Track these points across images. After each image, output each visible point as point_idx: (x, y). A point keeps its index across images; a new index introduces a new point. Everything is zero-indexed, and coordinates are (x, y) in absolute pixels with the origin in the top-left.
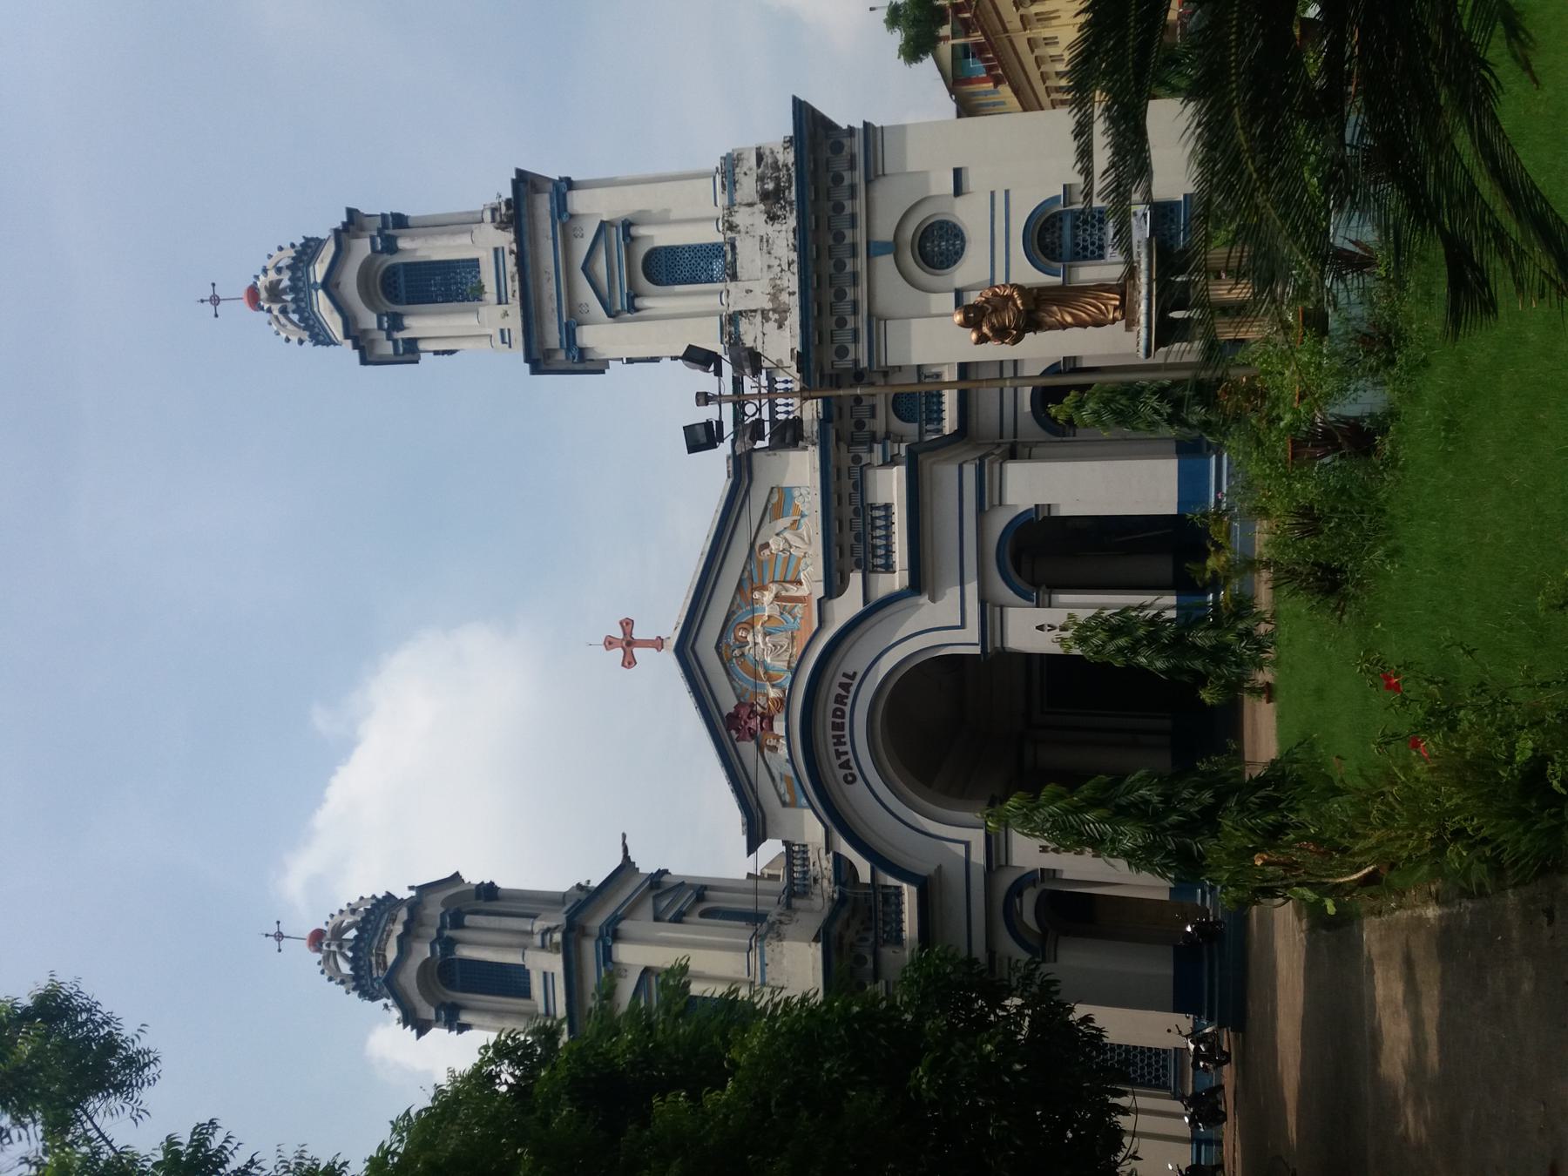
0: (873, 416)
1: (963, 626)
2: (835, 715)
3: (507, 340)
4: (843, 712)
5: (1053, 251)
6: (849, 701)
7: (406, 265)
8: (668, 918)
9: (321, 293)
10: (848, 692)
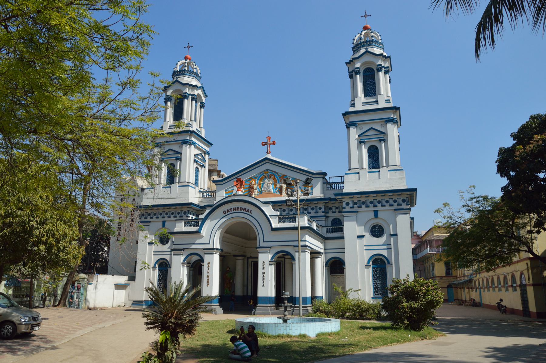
0: (333, 212)
1: (264, 242)
2: (241, 208)
4: (242, 210)
5: (375, 262)
6: (244, 212)
8: (195, 158)
9: (364, 50)
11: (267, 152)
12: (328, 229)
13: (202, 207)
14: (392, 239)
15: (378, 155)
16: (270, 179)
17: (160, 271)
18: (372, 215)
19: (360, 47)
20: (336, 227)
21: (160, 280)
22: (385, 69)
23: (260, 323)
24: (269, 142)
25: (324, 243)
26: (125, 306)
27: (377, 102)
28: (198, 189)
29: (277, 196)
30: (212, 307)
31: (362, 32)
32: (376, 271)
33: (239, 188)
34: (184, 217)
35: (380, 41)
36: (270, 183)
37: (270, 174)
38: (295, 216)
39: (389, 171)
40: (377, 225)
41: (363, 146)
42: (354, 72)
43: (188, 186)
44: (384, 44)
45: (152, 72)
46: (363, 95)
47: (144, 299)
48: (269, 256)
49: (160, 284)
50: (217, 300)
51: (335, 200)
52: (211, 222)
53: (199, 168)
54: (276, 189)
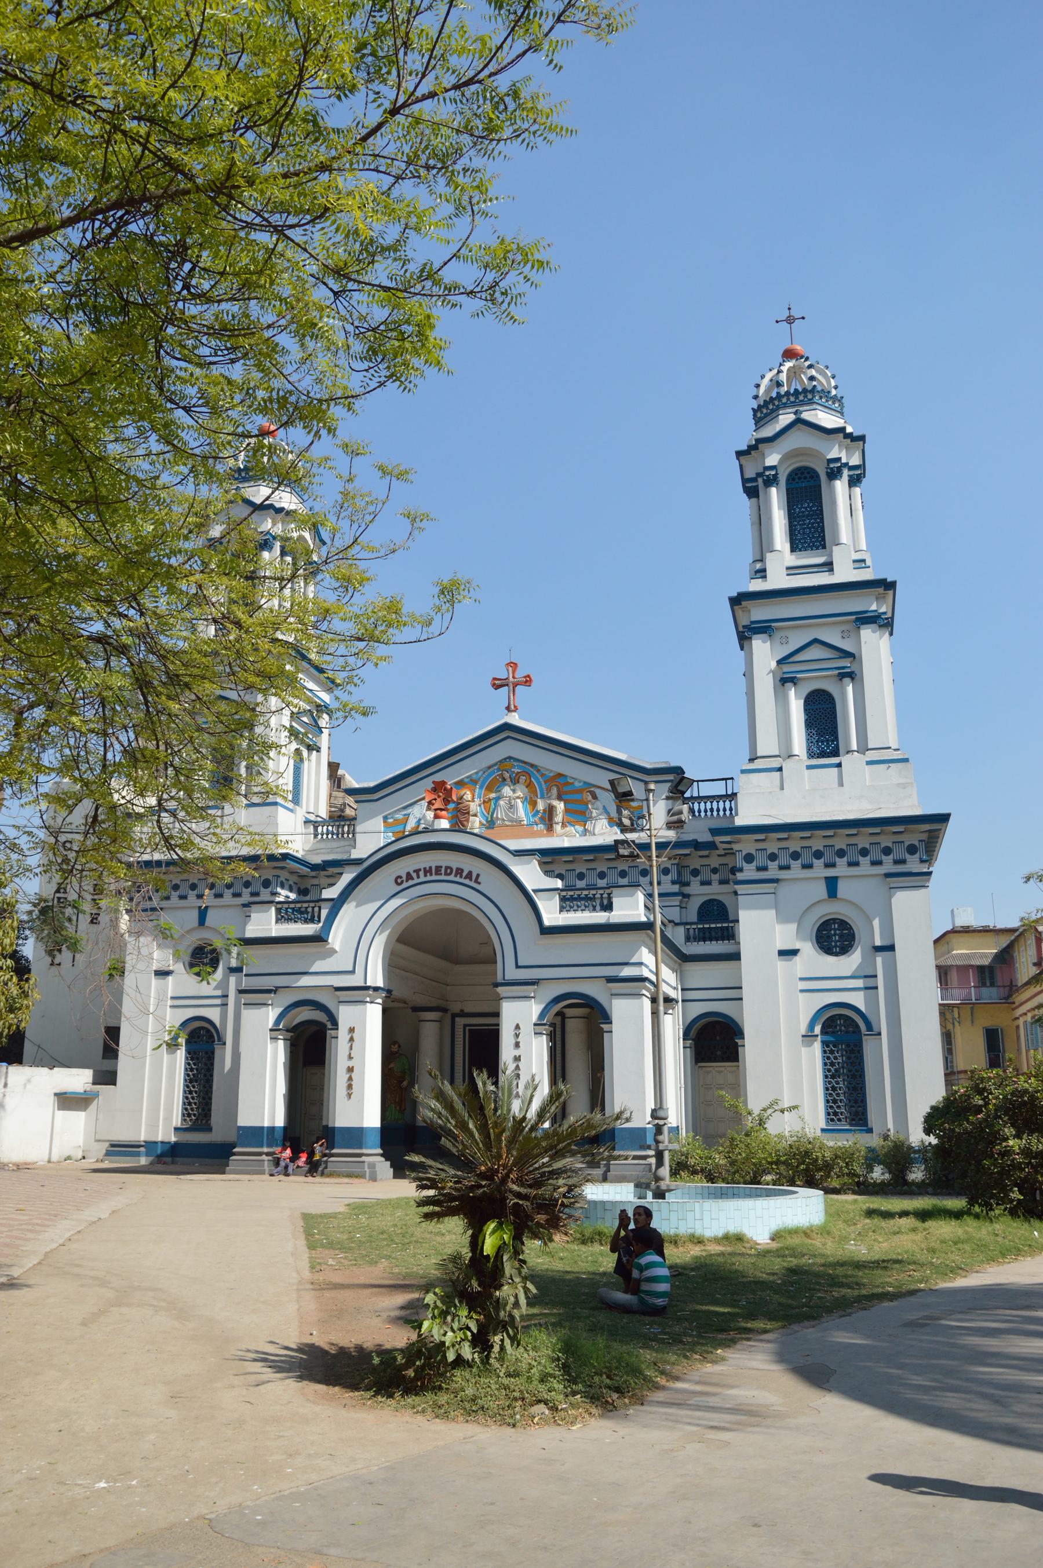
0: (703, 883)
1: (517, 967)
2: (447, 868)
3: (758, 575)
4: (450, 874)
5: (830, 1026)
6: (458, 879)
7: (820, 486)
8: (294, 724)
9: (791, 417)
10: (466, 878)
11: (508, 709)
12: (691, 931)
13: (314, 867)
14: (879, 960)
15: (835, 717)
16: (517, 786)
17: (191, 1054)
18: (820, 890)
19: (778, 408)
20: (713, 926)
21: (191, 1081)
22: (851, 473)
23: (603, 1203)
24: (514, 677)
25: (681, 971)
26: (84, 1158)
27: (829, 566)
28: (301, 813)
29: (538, 835)
30: (364, 1158)
31: (781, 365)
32: (832, 1052)
33: (441, 810)
34: (265, 895)
35: (834, 392)
36: (518, 798)
37: (516, 770)
39: (869, 763)
40: (834, 920)
41: (792, 693)
42: (760, 480)
43: (276, 804)
44: (844, 401)
45: (346, 440)
46: (787, 546)
47: (142, 1138)
48: (535, 1009)
49: (191, 1092)
50: (377, 1139)
51: (711, 846)
52: (359, 908)
53: (305, 753)
54: (533, 816)
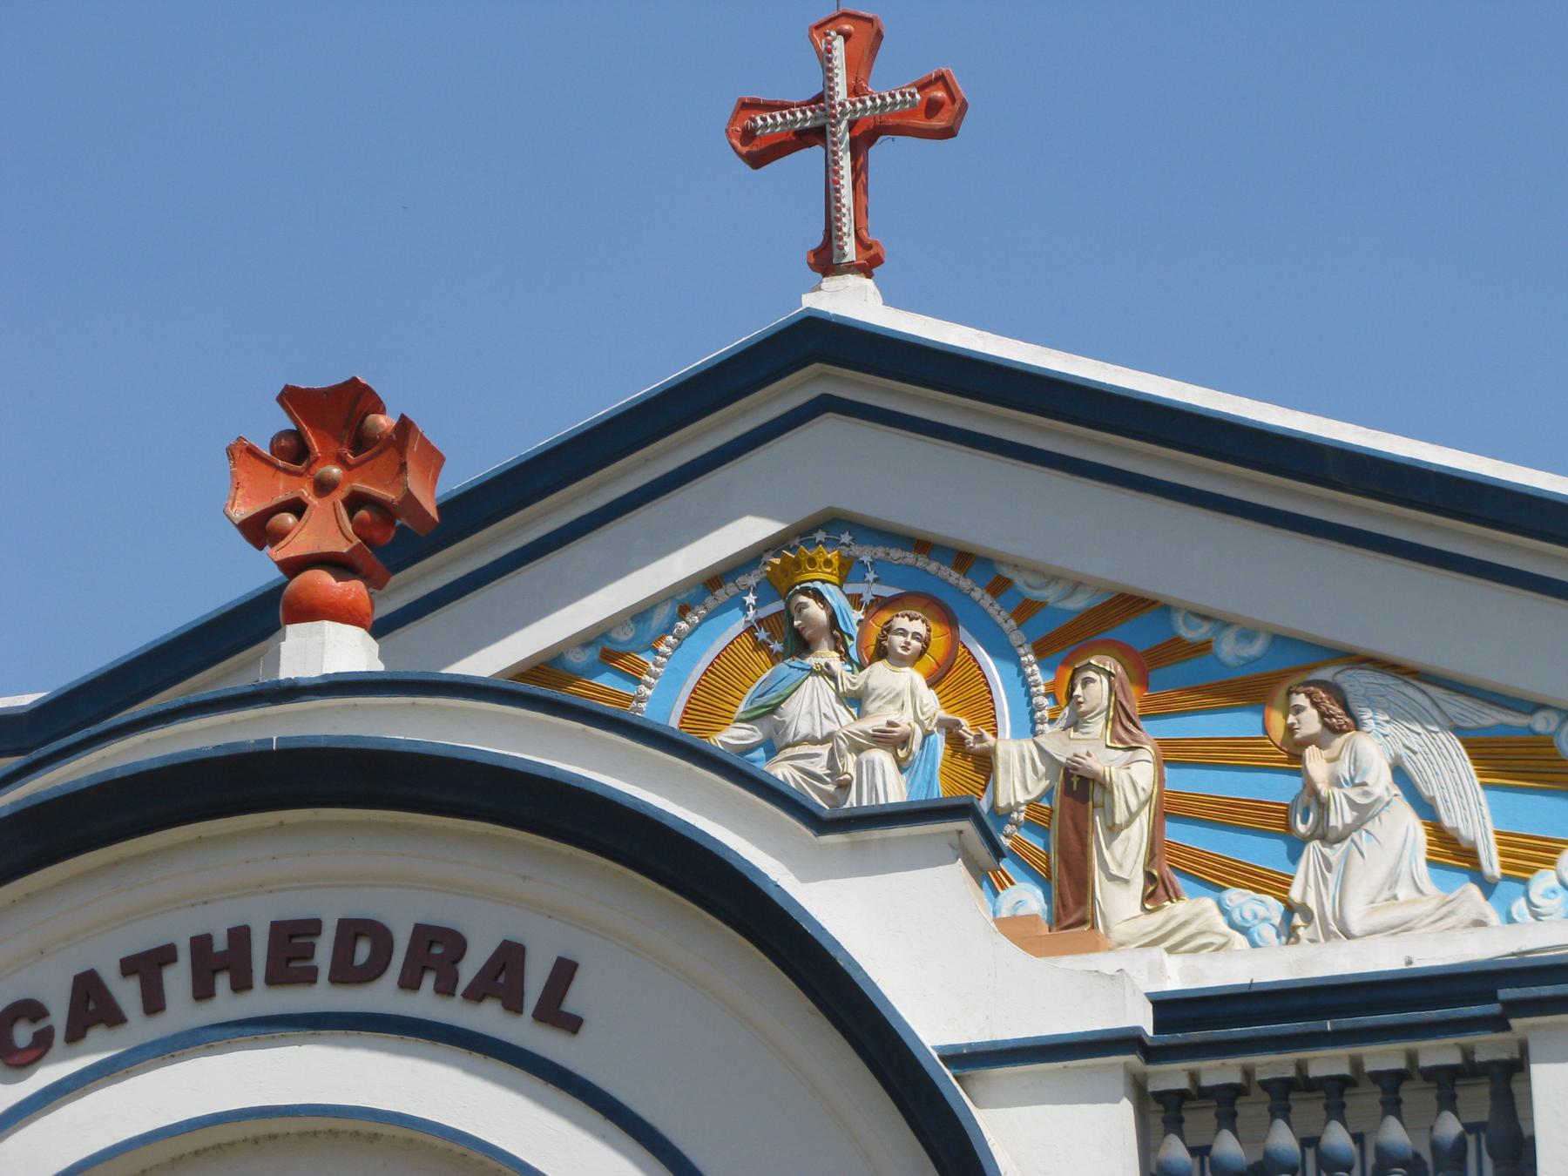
2: (351, 930)
4: (372, 972)
6: (425, 1004)
10: (476, 994)
24: (855, 91)
38: (1489, 1047)
